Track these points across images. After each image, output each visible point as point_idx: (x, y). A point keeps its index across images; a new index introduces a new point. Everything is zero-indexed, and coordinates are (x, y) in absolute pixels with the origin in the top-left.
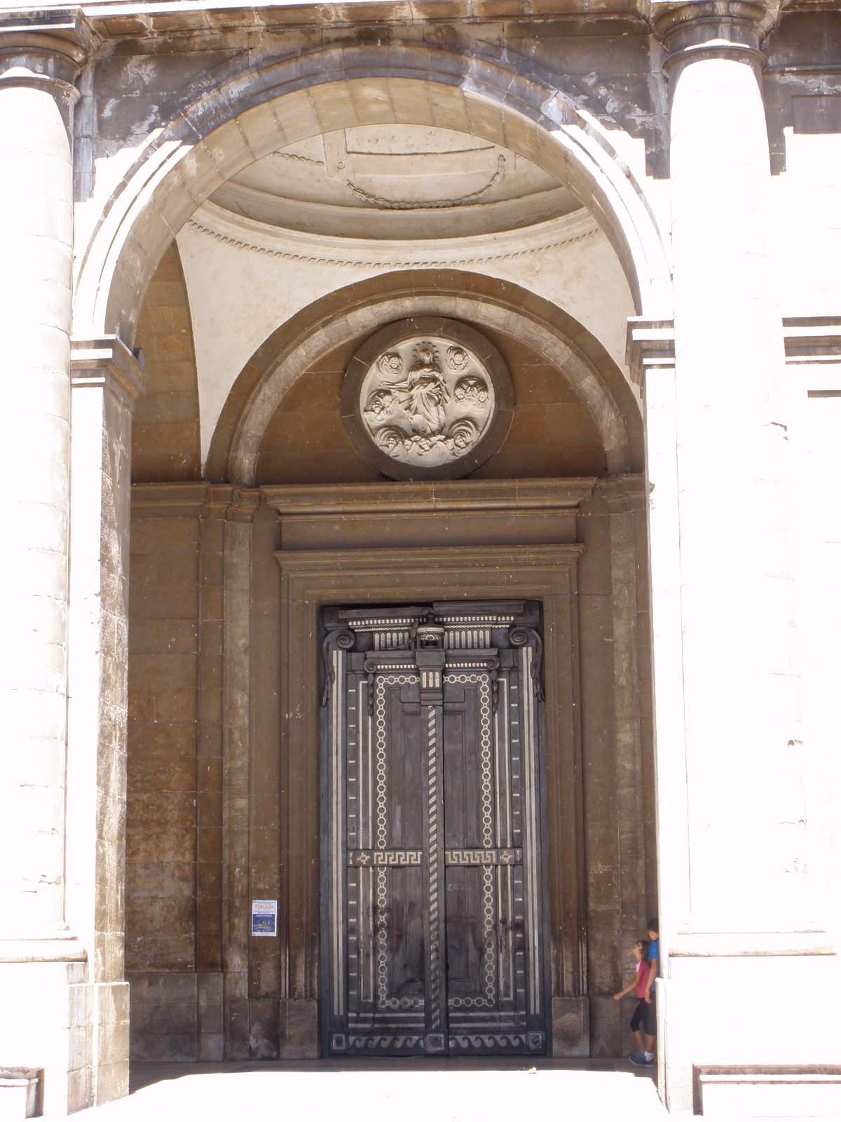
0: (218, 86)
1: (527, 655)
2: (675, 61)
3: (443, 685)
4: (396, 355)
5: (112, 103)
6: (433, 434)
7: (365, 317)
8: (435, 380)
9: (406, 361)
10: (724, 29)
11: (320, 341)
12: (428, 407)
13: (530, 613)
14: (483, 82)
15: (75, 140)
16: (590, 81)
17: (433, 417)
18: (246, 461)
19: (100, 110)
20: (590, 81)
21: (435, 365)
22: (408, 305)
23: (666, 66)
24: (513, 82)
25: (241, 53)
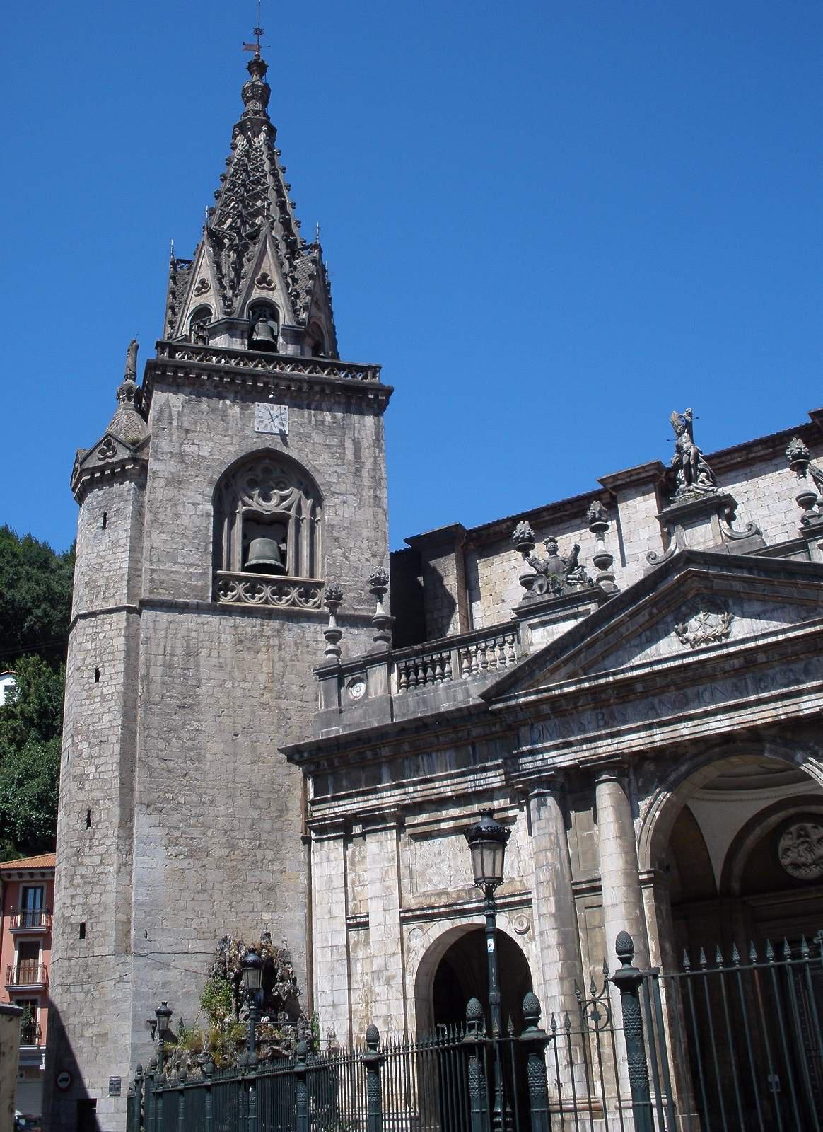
0: (677, 769)
4: (791, 833)
5: (641, 780)
6: (811, 864)
7: (775, 819)
8: (807, 842)
9: (795, 835)
11: (758, 831)
14: (771, 751)
16: (811, 744)
17: (809, 858)
18: (736, 886)
19: (637, 784)
21: (807, 835)
22: (792, 811)
25: (684, 754)
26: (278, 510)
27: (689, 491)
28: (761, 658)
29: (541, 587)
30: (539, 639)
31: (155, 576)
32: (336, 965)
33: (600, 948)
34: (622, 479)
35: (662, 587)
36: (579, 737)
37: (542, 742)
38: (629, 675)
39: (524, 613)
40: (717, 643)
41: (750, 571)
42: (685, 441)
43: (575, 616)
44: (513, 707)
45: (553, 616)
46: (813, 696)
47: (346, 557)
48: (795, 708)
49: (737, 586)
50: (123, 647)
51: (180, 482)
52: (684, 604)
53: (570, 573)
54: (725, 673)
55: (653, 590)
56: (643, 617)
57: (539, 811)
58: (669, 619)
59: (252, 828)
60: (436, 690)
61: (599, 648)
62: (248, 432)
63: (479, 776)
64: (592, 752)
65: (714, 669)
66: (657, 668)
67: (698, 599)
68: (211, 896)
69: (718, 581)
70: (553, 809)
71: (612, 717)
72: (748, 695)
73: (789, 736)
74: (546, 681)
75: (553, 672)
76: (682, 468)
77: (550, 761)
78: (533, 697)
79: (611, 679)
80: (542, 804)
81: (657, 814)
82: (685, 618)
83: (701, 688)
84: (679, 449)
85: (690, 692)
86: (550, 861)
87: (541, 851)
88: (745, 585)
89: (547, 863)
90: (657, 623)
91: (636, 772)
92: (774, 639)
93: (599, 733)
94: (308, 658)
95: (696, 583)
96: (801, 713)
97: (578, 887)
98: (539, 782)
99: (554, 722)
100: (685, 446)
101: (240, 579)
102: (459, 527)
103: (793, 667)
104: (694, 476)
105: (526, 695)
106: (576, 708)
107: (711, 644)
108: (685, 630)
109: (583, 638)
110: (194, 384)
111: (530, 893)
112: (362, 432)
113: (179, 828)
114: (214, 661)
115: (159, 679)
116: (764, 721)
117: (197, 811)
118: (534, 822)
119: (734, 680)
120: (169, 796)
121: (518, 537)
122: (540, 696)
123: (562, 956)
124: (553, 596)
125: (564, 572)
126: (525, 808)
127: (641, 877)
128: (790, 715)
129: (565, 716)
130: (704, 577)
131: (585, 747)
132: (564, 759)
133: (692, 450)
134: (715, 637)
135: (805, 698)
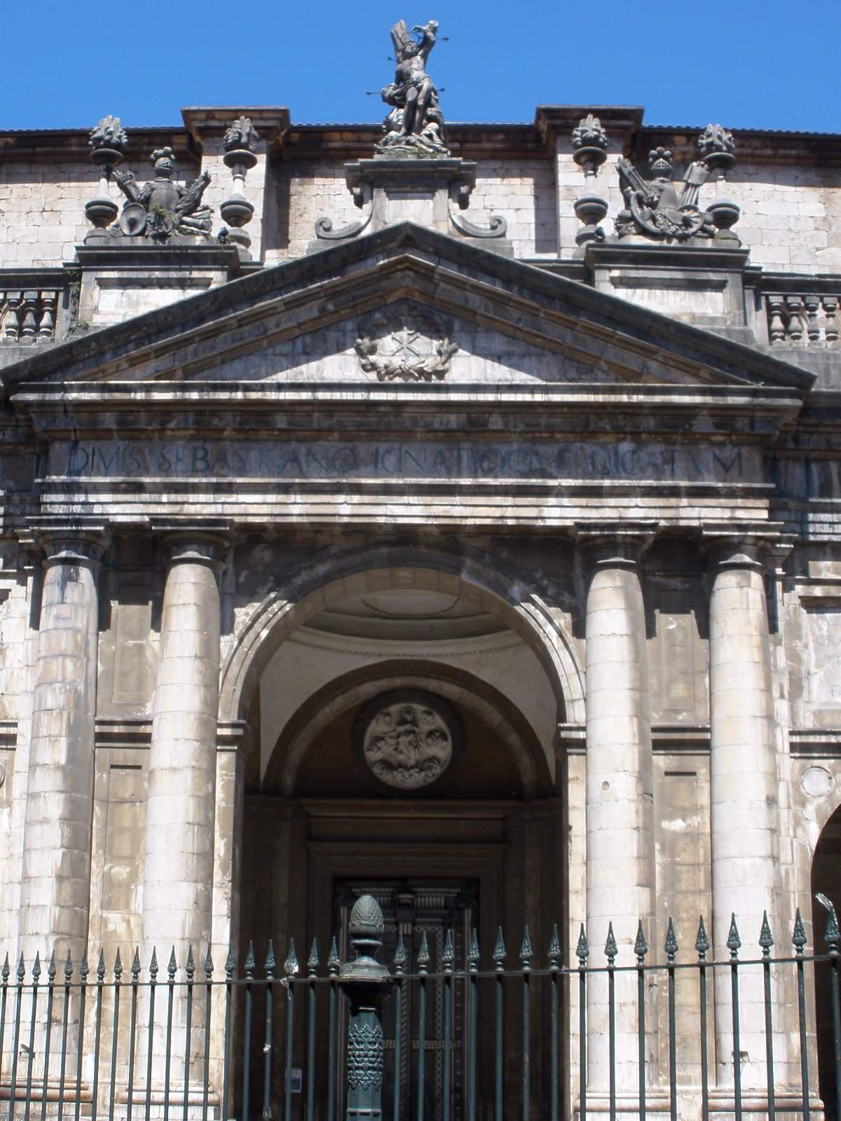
0: (311, 567)
1: (468, 914)
2: (591, 569)
3: (413, 932)
4: (388, 714)
5: (244, 574)
6: (412, 767)
7: (370, 688)
8: (414, 732)
9: (395, 719)
10: (621, 551)
11: (339, 703)
12: (409, 750)
13: (470, 889)
14: (474, 573)
15: (222, 595)
17: (412, 756)
18: (289, 780)
19: (237, 578)
20: (538, 575)
21: (414, 722)
22: (398, 682)
23: (585, 570)
24: (492, 574)
25: (326, 547)
27: (408, 143)
28: (496, 422)
29: (132, 224)
30: (110, 306)
33: (127, 836)
34: (218, 120)
35: (357, 271)
36: (158, 480)
37: (87, 474)
38: (272, 396)
39: (91, 259)
40: (422, 381)
41: (507, 283)
42: (416, 68)
43: (182, 284)
44: (53, 404)
45: (145, 275)
46: (566, 501)
48: (532, 512)
49: (476, 301)
52: (378, 308)
53: (188, 214)
54: (428, 432)
55: (339, 271)
56: (309, 312)
57: (63, 589)
58: (350, 326)
61: (223, 343)
64: (176, 509)
65: (415, 422)
66: (322, 395)
67: (404, 308)
69: (449, 287)
70: (87, 590)
71: (222, 459)
72: (460, 475)
73: (504, 555)
74: (118, 372)
75: (134, 362)
76: (401, 107)
77: (97, 509)
78: (94, 396)
79: (239, 395)
80: (68, 579)
81: (264, 634)
82: (376, 331)
83: (383, 447)
84: (402, 77)
85: (363, 448)
86: (69, 676)
87: (56, 656)
88: (490, 303)
89: (64, 679)
90: (327, 327)
91: (246, 557)
92: (527, 397)
93: (196, 480)
95: (408, 281)
96: (540, 523)
97: (107, 729)
98: (72, 540)
99: (114, 447)
100: (415, 75)
103: (541, 449)
104: (416, 124)
105: (82, 389)
106: (163, 430)
107: (411, 381)
108: (373, 350)
109: (202, 320)
111: (15, 725)
116: (478, 522)
118: (50, 605)
119: (441, 447)
121: (100, 139)
122: (107, 396)
123: (65, 841)
124: (151, 243)
125: (177, 211)
126: (30, 580)
127: (221, 732)
128: (522, 522)
129: (138, 439)
130: (426, 274)
131: (165, 498)
132: (125, 510)
133: (426, 85)
134: (421, 372)
135: (552, 501)
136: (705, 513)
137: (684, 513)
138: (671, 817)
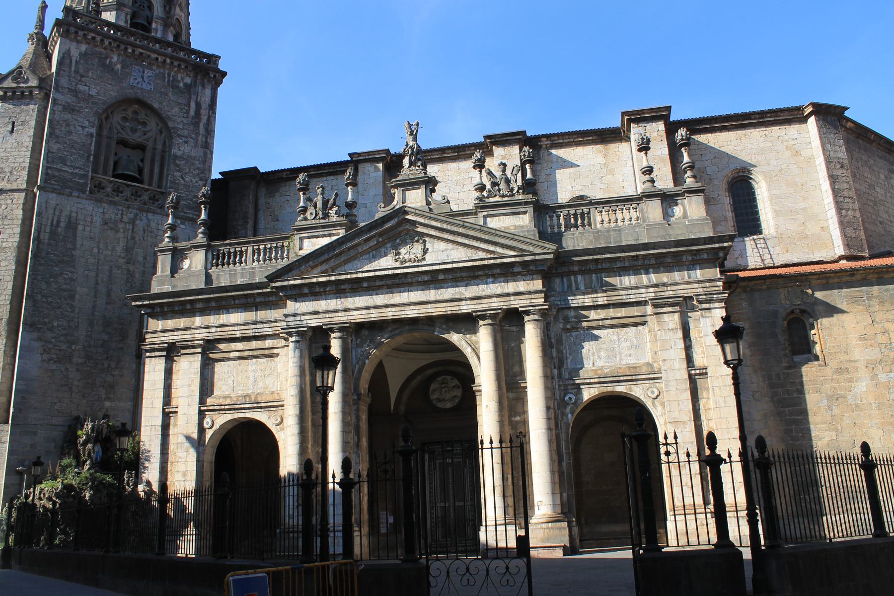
7: (430, 372)
17: (448, 396)
18: (402, 409)
26: (140, 140)
31: (49, 171)
32: (153, 438)
38: (360, 275)
43: (330, 235)
47: (183, 179)
50: (20, 217)
51: (73, 110)
56: (373, 243)
58: (389, 245)
59: (102, 346)
60: (235, 270)
62: (125, 85)
63: (258, 326)
66: (378, 273)
68: (71, 388)
77: (305, 322)
94: (150, 239)
101: (111, 182)
102: (255, 169)
110: (89, 43)
112: (203, 99)
113: (51, 342)
114: (87, 233)
115: (46, 241)
117: (65, 332)
120: (46, 320)
135: (463, 303)
136: (520, 302)
137: (512, 303)
138: (515, 416)
